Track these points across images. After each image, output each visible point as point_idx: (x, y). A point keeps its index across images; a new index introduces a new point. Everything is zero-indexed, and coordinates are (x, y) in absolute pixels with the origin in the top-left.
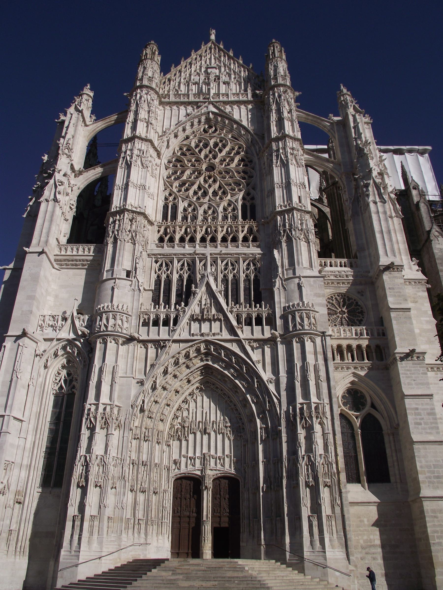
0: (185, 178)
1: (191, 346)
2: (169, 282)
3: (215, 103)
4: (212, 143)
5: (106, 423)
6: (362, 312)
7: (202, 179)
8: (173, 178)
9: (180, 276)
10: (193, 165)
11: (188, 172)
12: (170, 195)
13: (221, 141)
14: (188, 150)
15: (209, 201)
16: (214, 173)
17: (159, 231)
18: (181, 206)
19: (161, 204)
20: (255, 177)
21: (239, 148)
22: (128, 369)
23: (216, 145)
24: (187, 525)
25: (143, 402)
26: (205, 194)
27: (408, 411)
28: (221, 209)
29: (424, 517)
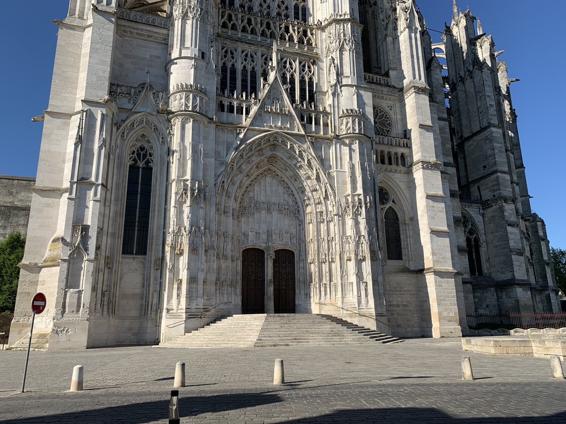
1: (265, 136)
2: (233, 71)
6: (389, 124)
17: (222, 17)
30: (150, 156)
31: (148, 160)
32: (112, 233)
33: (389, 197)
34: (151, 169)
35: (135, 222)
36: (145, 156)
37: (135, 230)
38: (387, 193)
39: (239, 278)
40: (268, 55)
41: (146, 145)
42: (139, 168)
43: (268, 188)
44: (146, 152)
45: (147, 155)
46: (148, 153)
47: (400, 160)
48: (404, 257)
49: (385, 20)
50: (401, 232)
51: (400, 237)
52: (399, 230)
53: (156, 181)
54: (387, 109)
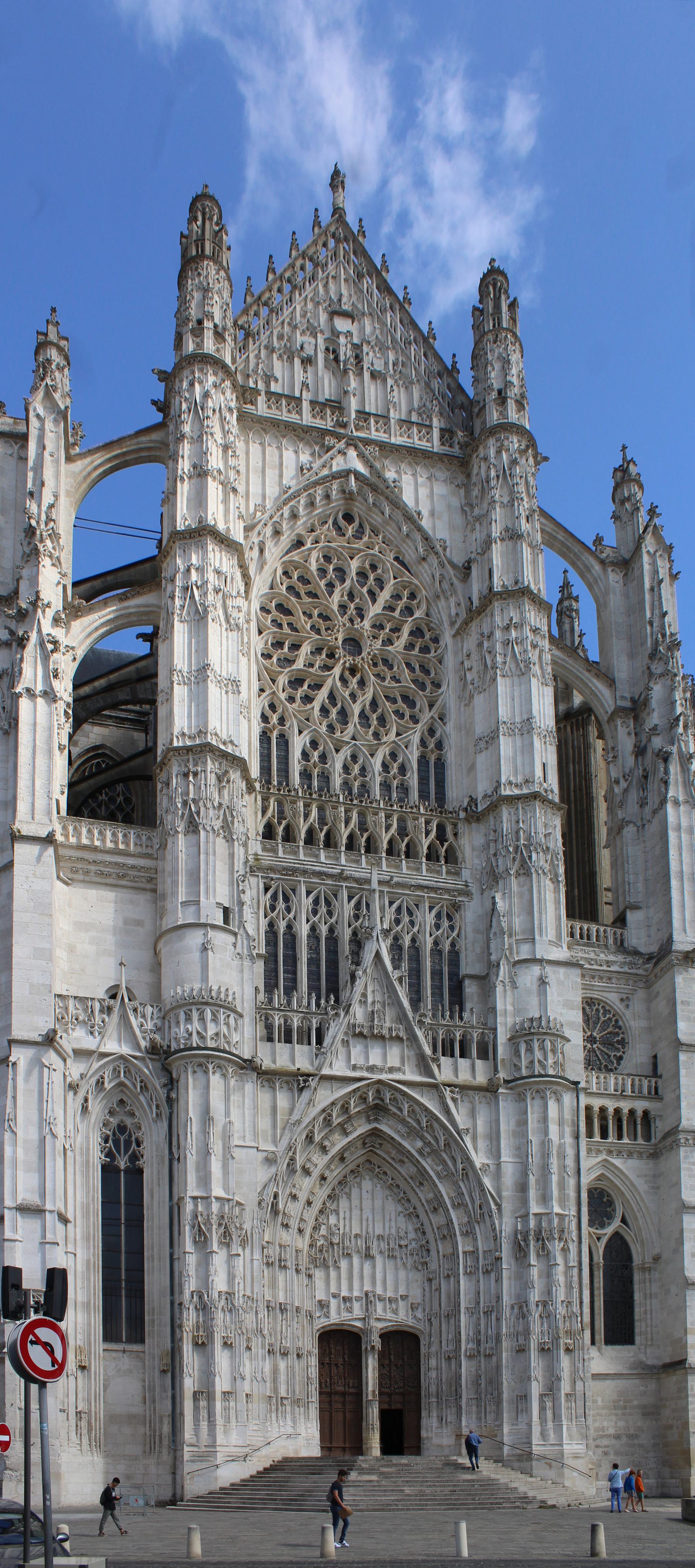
0: (301, 666)
3: (360, 445)
4: (354, 565)
5: (227, 1234)
7: (337, 671)
8: (275, 659)
9: (313, 929)
10: (315, 629)
11: (306, 649)
12: (272, 707)
13: (374, 567)
14: (301, 579)
15: (354, 738)
16: (363, 659)
18: (298, 743)
19: (257, 728)
20: (444, 688)
21: (412, 596)
22: (247, 1130)
23: (362, 575)
24: (340, 1406)
25: (276, 1196)
26: (344, 715)
27: (685, 1234)
28: (377, 764)
29: (687, 1396)
30: (138, 1144)
31: (134, 1151)
32: (83, 1303)
33: (614, 1210)
34: (140, 1172)
35: (120, 1281)
36: (128, 1143)
37: (121, 1296)
38: (611, 1203)
39: (314, 1388)
40: (361, 897)
41: (128, 1122)
42: (118, 1170)
43: (367, 1204)
44: (130, 1136)
45: (131, 1143)
46: (133, 1139)
47: (639, 1127)
48: (638, 1339)
49: (622, 780)
50: (636, 1287)
51: (632, 1297)
52: (631, 1282)
53: (152, 1197)
54: (619, 1006)
